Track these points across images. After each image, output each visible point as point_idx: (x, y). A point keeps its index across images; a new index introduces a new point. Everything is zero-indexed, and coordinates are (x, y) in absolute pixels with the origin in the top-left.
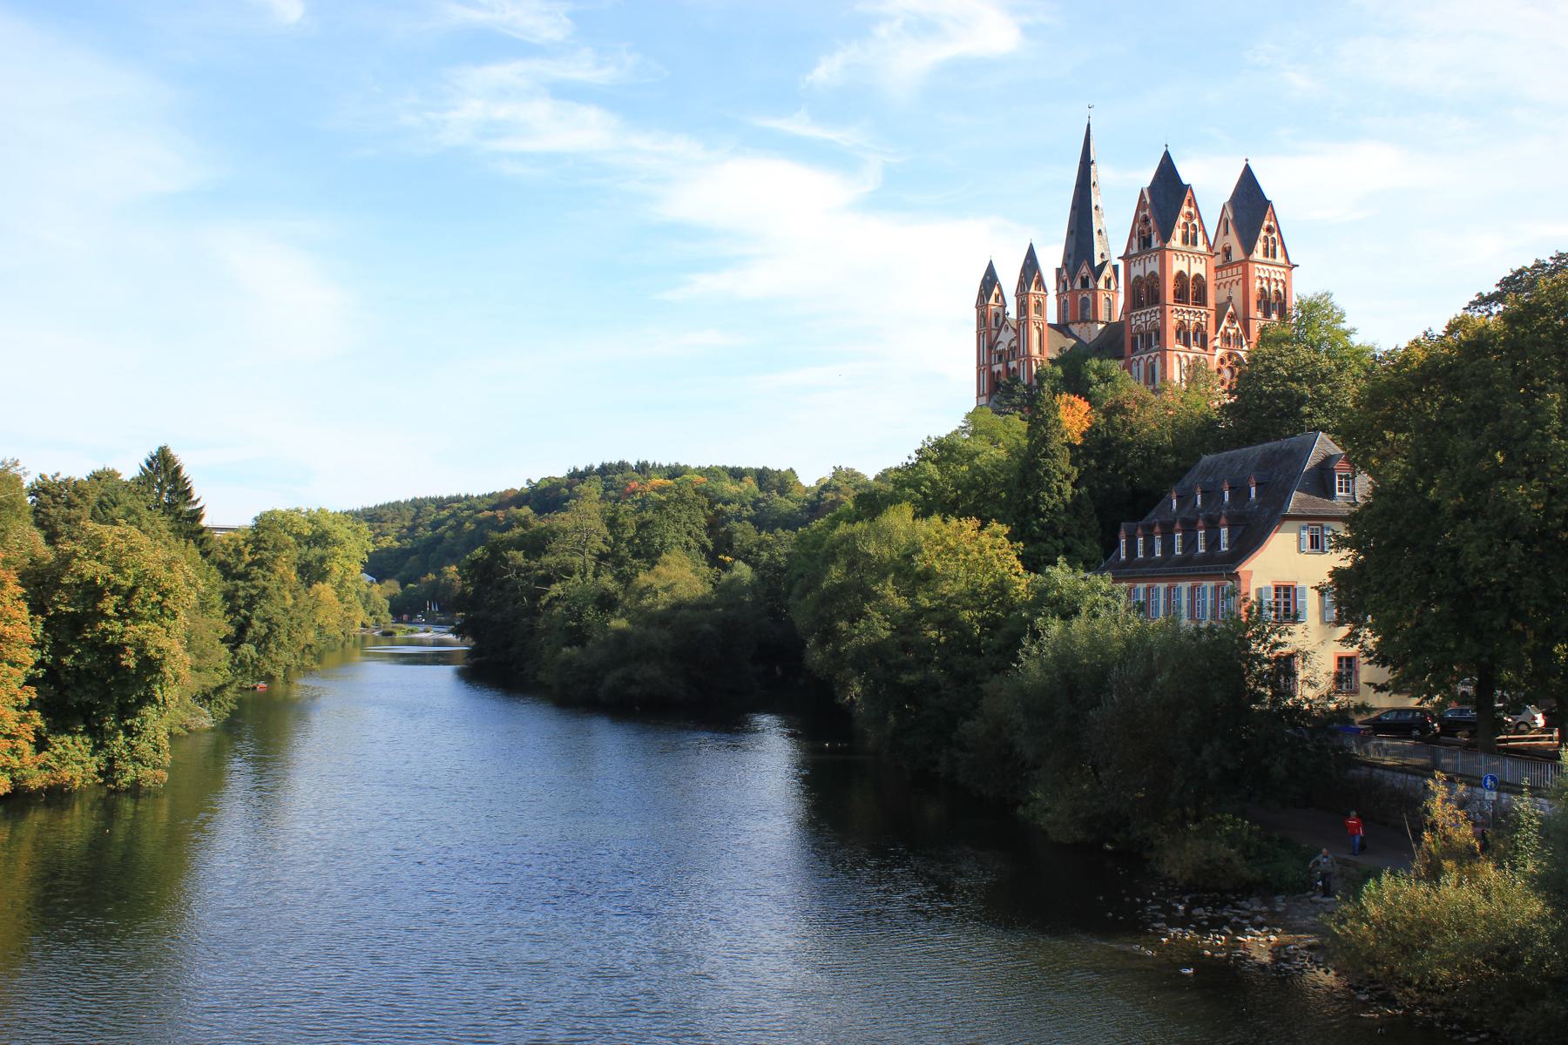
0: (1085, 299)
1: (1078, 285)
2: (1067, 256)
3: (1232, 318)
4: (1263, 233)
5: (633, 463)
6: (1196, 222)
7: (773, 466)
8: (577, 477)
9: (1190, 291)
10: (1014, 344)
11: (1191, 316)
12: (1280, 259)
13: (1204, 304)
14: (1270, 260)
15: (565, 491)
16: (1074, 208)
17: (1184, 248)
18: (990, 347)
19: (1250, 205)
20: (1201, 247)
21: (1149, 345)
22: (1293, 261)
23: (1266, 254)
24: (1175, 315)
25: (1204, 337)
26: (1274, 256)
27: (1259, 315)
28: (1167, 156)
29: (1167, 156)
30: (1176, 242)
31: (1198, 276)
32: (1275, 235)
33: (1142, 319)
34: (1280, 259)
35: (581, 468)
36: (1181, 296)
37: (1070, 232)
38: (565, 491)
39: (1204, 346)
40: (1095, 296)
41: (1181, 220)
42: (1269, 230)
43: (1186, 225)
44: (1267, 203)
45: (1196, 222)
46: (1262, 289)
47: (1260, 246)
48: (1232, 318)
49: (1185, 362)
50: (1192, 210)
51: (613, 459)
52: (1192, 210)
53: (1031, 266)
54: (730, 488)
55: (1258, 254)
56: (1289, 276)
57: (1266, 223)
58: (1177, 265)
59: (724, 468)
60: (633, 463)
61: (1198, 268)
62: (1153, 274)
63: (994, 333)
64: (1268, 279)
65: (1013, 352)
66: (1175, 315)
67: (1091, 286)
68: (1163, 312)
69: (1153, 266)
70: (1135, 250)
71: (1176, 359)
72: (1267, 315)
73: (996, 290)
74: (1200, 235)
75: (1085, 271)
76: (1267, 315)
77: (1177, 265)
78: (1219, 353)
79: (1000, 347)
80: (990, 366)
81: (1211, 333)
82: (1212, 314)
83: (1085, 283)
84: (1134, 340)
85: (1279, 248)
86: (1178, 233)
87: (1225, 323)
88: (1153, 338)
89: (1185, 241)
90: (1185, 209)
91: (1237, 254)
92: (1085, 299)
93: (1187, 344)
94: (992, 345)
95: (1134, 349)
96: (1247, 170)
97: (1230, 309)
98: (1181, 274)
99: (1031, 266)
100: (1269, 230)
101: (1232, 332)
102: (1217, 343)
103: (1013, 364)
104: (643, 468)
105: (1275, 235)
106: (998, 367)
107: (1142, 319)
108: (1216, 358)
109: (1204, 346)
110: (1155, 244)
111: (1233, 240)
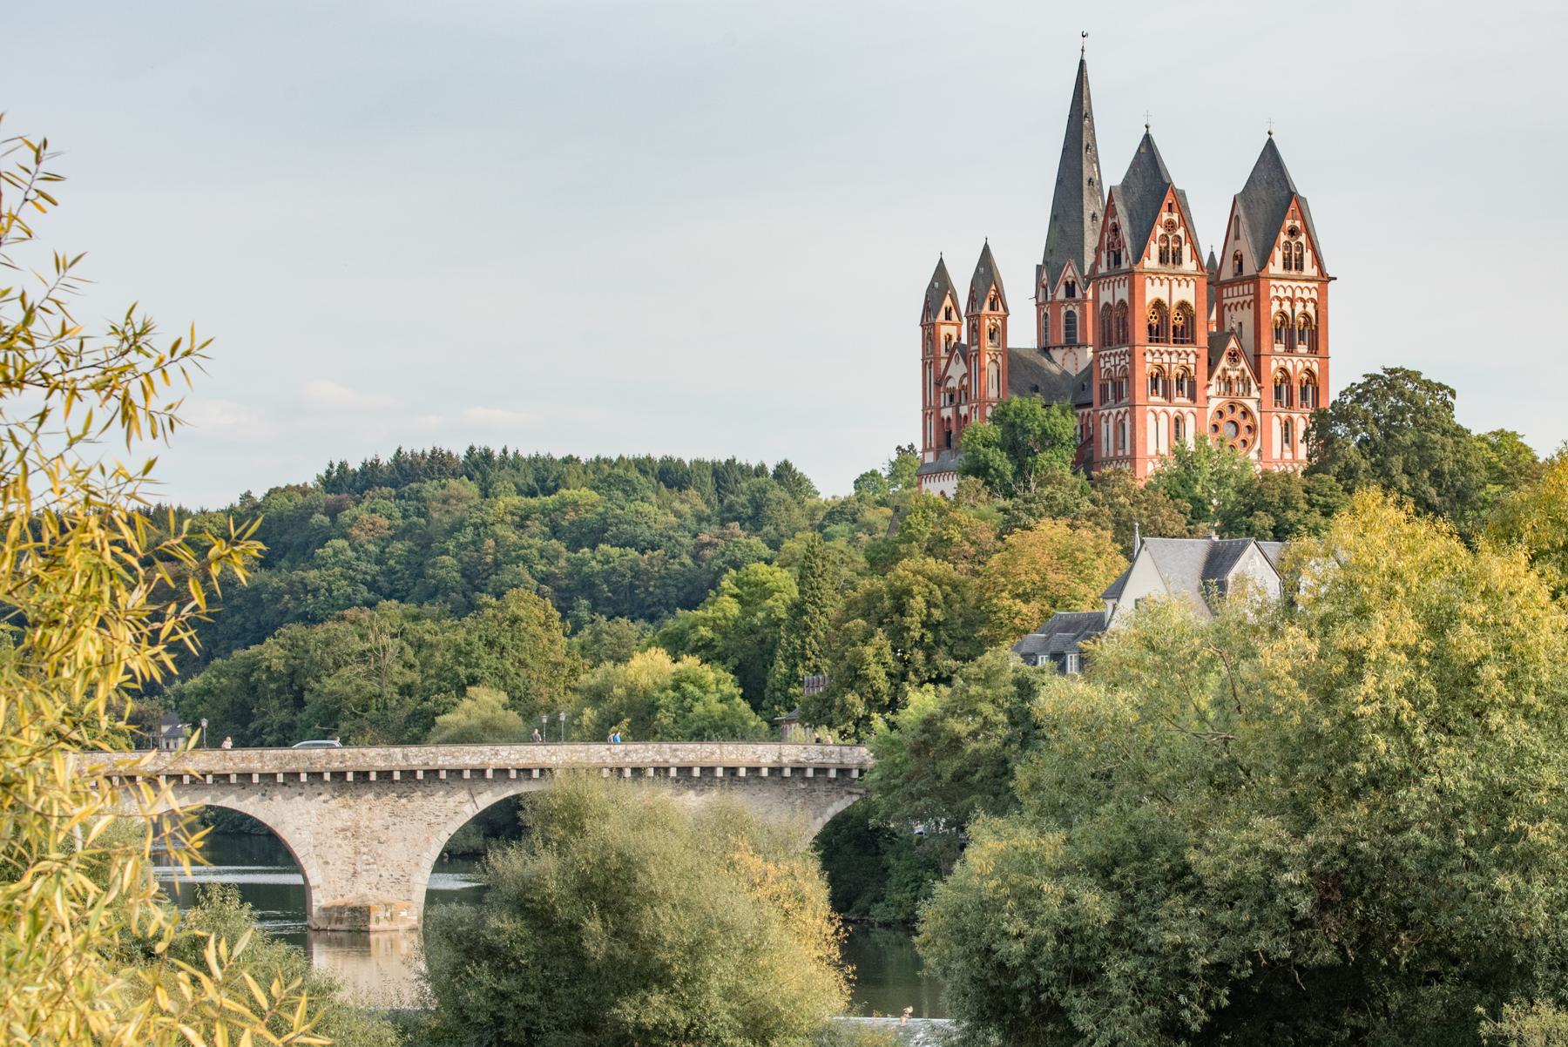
0: (1070, 314)
1: (1061, 294)
2: (1049, 251)
3: (1234, 357)
4: (1283, 237)
5: (460, 452)
6: (1181, 232)
7: (749, 457)
8: (340, 482)
9: (1172, 327)
10: (965, 382)
11: (1174, 358)
12: (1310, 270)
13: (1193, 342)
14: (1293, 272)
15: (320, 518)
16: (1059, 182)
17: (1163, 268)
18: (938, 384)
19: (1271, 199)
20: (1189, 265)
21: (1118, 396)
22: (1330, 272)
23: (1287, 266)
24: (1150, 358)
25: (1193, 384)
26: (1302, 269)
27: (1280, 348)
28: (1147, 138)
29: (1147, 138)
30: (1151, 262)
31: (1183, 305)
32: (1303, 239)
33: (1112, 362)
34: (1310, 270)
35: (355, 465)
36: (1156, 334)
37: (1054, 218)
38: (320, 518)
39: (1192, 396)
40: (1083, 309)
41: (1159, 231)
42: (1293, 232)
43: (1164, 238)
44: (1291, 195)
45: (1181, 232)
46: (1283, 313)
47: (1278, 255)
48: (1234, 357)
49: (1163, 417)
50: (1175, 217)
51: (419, 444)
52: (1175, 217)
53: (986, 270)
54: (655, 512)
55: (1276, 267)
56: (1323, 293)
57: (1288, 223)
58: (1154, 291)
59: (643, 465)
60: (460, 452)
61: (1186, 293)
62: (1122, 302)
63: (943, 363)
64: (1292, 301)
65: (965, 389)
66: (1150, 358)
67: (1078, 295)
68: (1131, 354)
69: (1122, 293)
70: (1103, 269)
71: (1151, 416)
72: (1290, 348)
73: (948, 302)
74: (1186, 250)
75: (1070, 272)
76: (1290, 348)
77: (1154, 291)
78: (1215, 404)
79: (950, 384)
80: (939, 409)
81: (1201, 379)
82: (1204, 354)
83: (1070, 290)
84: (1104, 388)
85: (1308, 256)
86: (1154, 248)
87: (1224, 363)
88: (1119, 388)
89: (1163, 259)
90: (1165, 216)
91: (1250, 268)
92: (1070, 314)
93: (1165, 396)
94: (940, 381)
95: (1104, 399)
96: (1270, 145)
97: (1233, 344)
98: (1158, 304)
99: (986, 270)
100: (1293, 232)
101: (1233, 374)
102: (1211, 391)
103: (964, 410)
104: (480, 466)
105: (1303, 239)
106: (947, 413)
107: (1112, 362)
108: (1210, 412)
109: (1192, 396)
110: (1125, 266)
111: (1246, 247)
